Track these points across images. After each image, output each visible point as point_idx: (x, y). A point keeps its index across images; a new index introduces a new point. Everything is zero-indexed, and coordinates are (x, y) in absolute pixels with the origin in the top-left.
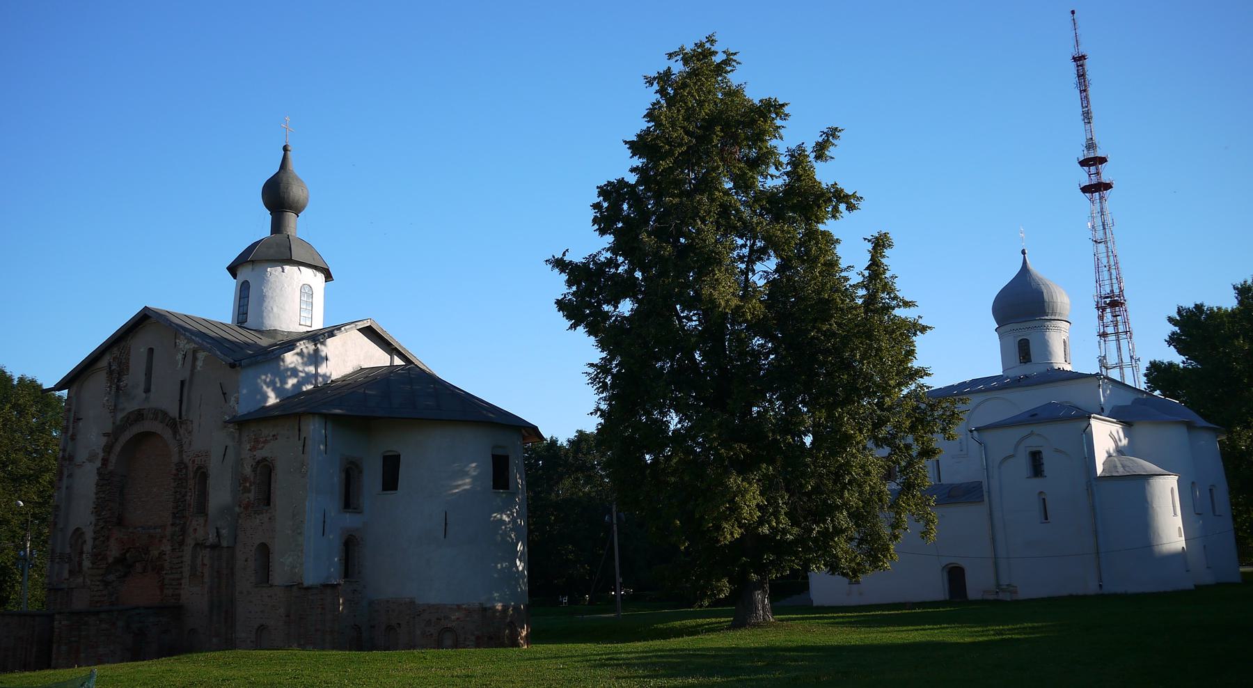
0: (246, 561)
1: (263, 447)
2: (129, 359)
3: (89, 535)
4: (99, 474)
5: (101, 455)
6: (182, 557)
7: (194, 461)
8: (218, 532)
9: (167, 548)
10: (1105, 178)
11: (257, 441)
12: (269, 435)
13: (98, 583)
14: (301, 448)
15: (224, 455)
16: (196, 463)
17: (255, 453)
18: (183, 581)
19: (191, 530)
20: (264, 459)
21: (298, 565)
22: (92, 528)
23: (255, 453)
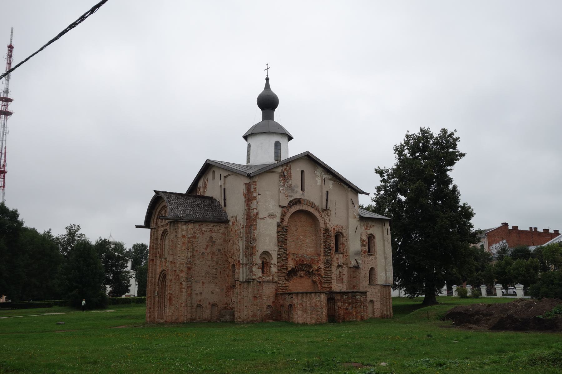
0: (365, 274)
1: (369, 229)
2: (291, 172)
3: (275, 256)
4: (279, 225)
5: (279, 216)
6: (331, 270)
7: (334, 229)
8: (357, 262)
9: (322, 266)
10: (10, 109)
11: (367, 226)
12: (371, 225)
13: (284, 280)
14: (386, 232)
15: (356, 229)
18: (332, 281)
19: (335, 259)
20: (371, 234)
21: (391, 277)
22: (276, 253)
23: (367, 231)
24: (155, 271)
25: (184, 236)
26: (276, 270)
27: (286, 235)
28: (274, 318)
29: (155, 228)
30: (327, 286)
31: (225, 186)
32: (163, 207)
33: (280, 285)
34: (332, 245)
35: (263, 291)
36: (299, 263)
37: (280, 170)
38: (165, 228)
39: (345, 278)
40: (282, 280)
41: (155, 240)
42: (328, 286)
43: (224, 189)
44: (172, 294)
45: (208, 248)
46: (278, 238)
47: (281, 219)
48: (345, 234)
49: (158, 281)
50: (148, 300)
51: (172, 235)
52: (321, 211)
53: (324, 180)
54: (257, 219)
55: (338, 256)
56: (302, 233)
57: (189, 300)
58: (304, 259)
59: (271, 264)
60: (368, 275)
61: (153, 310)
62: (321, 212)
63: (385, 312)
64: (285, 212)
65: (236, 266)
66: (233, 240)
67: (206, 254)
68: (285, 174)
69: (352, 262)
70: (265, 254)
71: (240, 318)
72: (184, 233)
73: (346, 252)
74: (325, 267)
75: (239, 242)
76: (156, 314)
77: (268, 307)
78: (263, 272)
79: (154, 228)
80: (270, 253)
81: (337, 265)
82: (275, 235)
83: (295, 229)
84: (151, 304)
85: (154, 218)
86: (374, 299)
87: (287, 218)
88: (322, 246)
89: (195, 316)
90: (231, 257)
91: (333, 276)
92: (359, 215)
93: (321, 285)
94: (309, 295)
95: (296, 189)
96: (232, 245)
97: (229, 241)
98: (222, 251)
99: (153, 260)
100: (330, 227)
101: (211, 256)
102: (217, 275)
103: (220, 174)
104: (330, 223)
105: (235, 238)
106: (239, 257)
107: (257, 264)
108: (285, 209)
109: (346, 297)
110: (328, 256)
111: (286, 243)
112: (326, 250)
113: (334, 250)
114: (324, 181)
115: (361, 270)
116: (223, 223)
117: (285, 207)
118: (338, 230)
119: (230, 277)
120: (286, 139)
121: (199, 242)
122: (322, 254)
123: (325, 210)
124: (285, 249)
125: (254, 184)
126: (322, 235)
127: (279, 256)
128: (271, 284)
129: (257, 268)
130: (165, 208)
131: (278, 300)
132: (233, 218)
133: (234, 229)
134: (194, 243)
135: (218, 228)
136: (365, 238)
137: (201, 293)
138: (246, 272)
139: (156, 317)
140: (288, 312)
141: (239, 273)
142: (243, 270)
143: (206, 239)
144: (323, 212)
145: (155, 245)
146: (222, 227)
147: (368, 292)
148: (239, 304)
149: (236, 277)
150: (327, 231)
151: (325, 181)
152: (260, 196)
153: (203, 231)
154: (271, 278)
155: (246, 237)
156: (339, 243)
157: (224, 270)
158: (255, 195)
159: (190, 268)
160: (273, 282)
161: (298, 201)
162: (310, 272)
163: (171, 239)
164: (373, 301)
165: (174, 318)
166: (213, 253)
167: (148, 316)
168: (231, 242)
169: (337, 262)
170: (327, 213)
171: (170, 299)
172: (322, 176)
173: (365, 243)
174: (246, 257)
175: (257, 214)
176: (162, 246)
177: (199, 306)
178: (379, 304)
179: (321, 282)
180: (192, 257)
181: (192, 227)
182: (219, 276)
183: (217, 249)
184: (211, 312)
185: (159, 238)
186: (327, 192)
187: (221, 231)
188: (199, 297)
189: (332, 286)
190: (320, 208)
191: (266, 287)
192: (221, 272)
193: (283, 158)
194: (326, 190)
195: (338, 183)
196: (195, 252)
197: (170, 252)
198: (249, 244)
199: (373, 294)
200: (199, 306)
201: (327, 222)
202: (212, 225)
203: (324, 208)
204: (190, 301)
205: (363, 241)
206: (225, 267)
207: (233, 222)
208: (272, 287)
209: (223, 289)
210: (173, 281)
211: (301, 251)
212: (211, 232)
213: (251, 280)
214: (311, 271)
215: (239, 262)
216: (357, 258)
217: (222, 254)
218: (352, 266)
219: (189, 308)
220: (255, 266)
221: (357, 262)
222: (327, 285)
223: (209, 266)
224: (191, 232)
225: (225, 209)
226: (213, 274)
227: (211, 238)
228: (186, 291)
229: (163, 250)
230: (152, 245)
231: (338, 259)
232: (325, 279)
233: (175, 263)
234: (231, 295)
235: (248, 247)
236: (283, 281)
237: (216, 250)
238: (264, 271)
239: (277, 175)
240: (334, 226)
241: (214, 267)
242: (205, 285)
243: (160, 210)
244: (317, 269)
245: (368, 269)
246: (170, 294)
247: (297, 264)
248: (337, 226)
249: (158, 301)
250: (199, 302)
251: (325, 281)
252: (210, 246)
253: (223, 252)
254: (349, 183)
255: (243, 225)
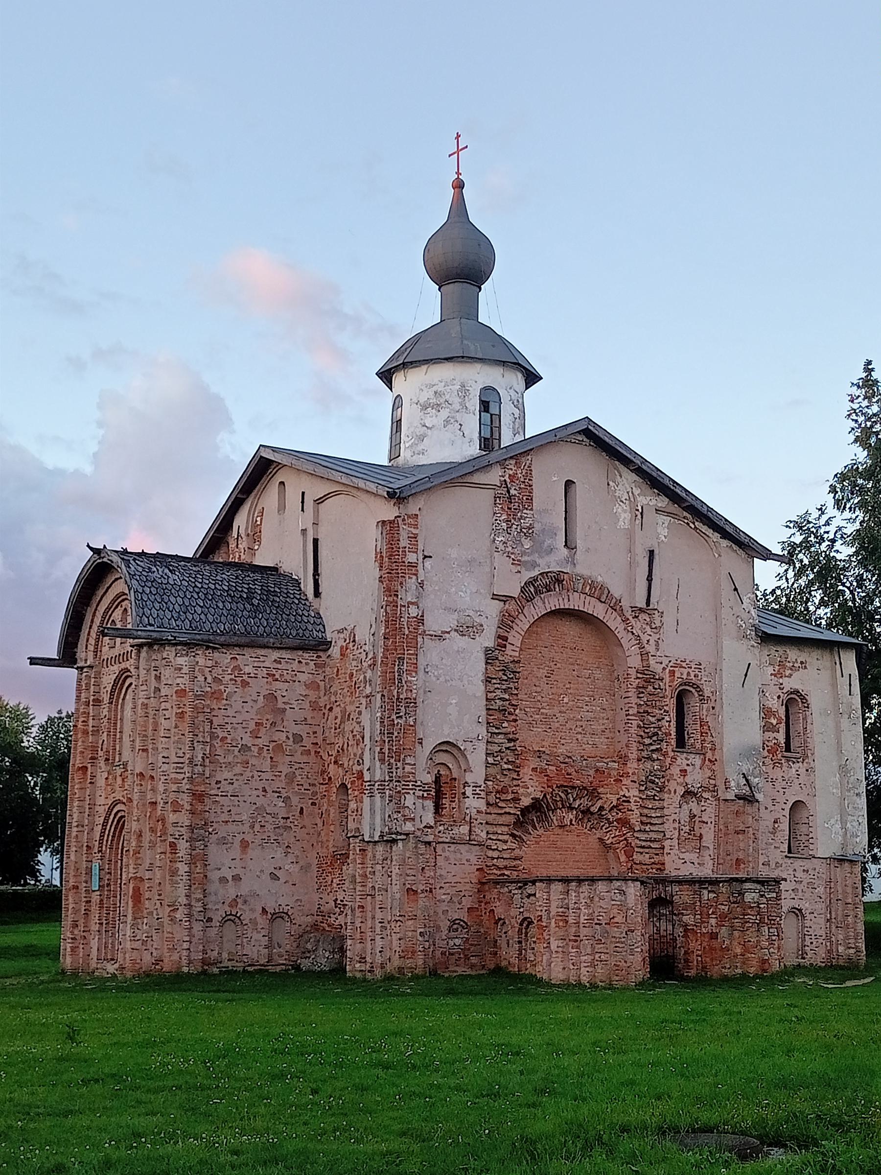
0: (774, 822)
1: (790, 676)
3: (477, 758)
4: (490, 658)
7: (672, 673)
8: (747, 780)
9: (633, 793)
13: (506, 837)
15: (746, 675)
16: (677, 675)
17: (781, 681)
18: (667, 843)
19: (675, 771)
20: (796, 692)
22: (482, 747)
23: (781, 681)
24: (92, 806)
25: (181, 693)
26: (481, 804)
27: (516, 692)
28: (474, 960)
29: (91, 667)
30: (648, 861)
31: (316, 531)
32: (118, 596)
33: (495, 854)
34: (667, 724)
35: (439, 872)
36: (555, 782)
37: (494, 476)
38: (123, 666)
39: (709, 839)
40: (500, 837)
41: (91, 703)
42: (652, 860)
43: (316, 542)
44: (142, 879)
45: (263, 731)
46: (487, 699)
47: (499, 637)
48: (707, 693)
49: (102, 836)
50: (67, 900)
51: (144, 688)
52: (628, 614)
53: (642, 513)
54: (420, 639)
55: (685, 762)
56: (568, 686)
57: (198, 900)
58: (572, 770)
59: (466, 784)
60: (785, 826)
61: (84, 931)
62: (630, 618)
63: (841, 949)
64: (510, 615)
65: (350, 792)
66: (342, 705)
67: (255, 750)
68: (513, 492)
69: (733, 784)
70: (446, 751)
71: (363, 960)
72: (183, 682)
73: (713, 750)
74: (644, 797)
75: (360, 713)
76: (94, 944)
77: (455, 926)
78: (438, 808)
79: (89, 667)
80: (462, 748)
81: (681, 790)
82: (479, 689)
83: (543, 672)
84: (76, 911)
85: (89, 634)
86: (805, 906)
87: (516, 635)
88: (634, 730)
89: (215, 953)
90: (336, 762)
91: (669, 827)
92: (757, 630)
93: (629, 855)
94: (585, 887)
95: (548, 542)
96: (338, 721)
97: (331, 709)
98: (307, 743)
99: (84, 769)
100: (658, 669)
101: (271, 758)
102: (289, 818)
103: (303, 493)
104: (658, 654)
105: (348, 699)
106: (361, 761)
107: (419, 783)
108: (511, 606)
109: (712, 895)
110: (654, 761)
111: (514, 717)
112: (647, 741)
113: (673, 742)
114: (639, 516)
115: (762, 808)
116: (311, 650)
117: (514, 598)
118: (685, 676)
119: (332, 828)
120: (518, 380)
121: (230, 712)
122: (633, 755)
123: (640, 609)
124: (511, 736)
125: (410, 525)
126: (632, 693)
127: (491, 760)
128: (463, 848)
129: (418, 797)
130: (123, 600)
131: (486, 904)
132: (342, 636)
133: (346, 668)
134: (213, 713)
135: (295, 665)
136: (774, 704)
137: (237, 878)
138: (383, 810)
139: (94, 953)
140: (520, 942)
141: (359, 813)
142: (372, 805)
143: (255, 701)
144: (636, 617)
145: (91, 723)
146: (307, 664)
147: (785, 880)
148: (358, 913)
149: (351, 825)
150: (648, 678)
151: (644, 516)
152: (428, 563)
153: (245, 677)
154: (465, 829)
155: (383, 695)
156: (688, 720)
157: (313, 804)
158: (411, 558)
159: (203, 795)
160: (469, 842)
161: (554, 582)
162: (592, 814)
163: (140, 701)
164: (800, 910)
165: (147, 959)
166: (279, 748)
167: (69, 950)
168: (337, 710)
169: (681, 780)
170: (648, 620)
171: (137, 897)
172: (632, 499)
173: (774, 722)
174: (382, 761)
175: (421, 620)
176: (115, 724)
177: (232, 918)
178: (822, 921)
179: (628, 844)
180: (207, 761)
181: (209, 664)
182: (296, 823)
183: (290, 736)
184: (270, 940)
185: (106, 698)
186: (652, 553)
187: (303, 677)
188: (231, 891)
189: (667, 859)
190: (626, 604)
191: (447, 859)
192: (302, 809)
193: (507, 439)
194: (649, 545)
195: (688, 524)
196: (220, 744)
197: (138, 744)
198: (394, 717)
199: (800, 887)
200: (232, 918)
201: (651, 648)
202: (276, 655)
203: (643, 605)
204: (200, 904)
205: (767, 712)
206: (315, 794)
207: (342, 647)
208: (467, 860)
209: (309, 865)
210: (147, 836)
211: (563, 745)
212: (270, 679)
213: (399, 837)
214: (594, 809)
215: (360, 775)
216: (746, 767)
217: (308, 752)
218: (730, 796)
219: (197, 927)
220: (411, 792)
221: (747, 780)
222: (647, 856)
223: (264, 790)
224: (206, 678)
225: (315, 603)
226: (274, 816)
227: (272, 697)
228: (187, 869)
229: (118, 737)
230: (83, 722)
231: (686, 771)
232: (643, 836)
233: (152, 777)
234: (335, 885)
235: (388, 727)
236: (506, 842)
237: (288, 738)
238: (442, 808)
239: (487, 496)
240: (671, 664)
241: (279, 792)
242: (250, 851)
243: (108, 608)
244: (615, 803)
245: (784, 806)
246: (136, 878)
247: (548, 787)
248: (684, 664)
249: (101, 900)
250: (230, 906)
251: (644, 844)
252: (268, 726)
253: (309, 746)
254: (721, 524)
255: (374, 658)
